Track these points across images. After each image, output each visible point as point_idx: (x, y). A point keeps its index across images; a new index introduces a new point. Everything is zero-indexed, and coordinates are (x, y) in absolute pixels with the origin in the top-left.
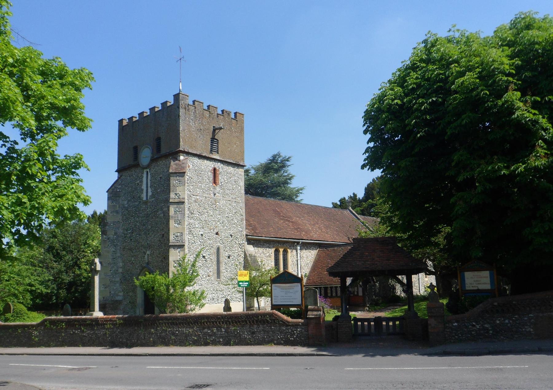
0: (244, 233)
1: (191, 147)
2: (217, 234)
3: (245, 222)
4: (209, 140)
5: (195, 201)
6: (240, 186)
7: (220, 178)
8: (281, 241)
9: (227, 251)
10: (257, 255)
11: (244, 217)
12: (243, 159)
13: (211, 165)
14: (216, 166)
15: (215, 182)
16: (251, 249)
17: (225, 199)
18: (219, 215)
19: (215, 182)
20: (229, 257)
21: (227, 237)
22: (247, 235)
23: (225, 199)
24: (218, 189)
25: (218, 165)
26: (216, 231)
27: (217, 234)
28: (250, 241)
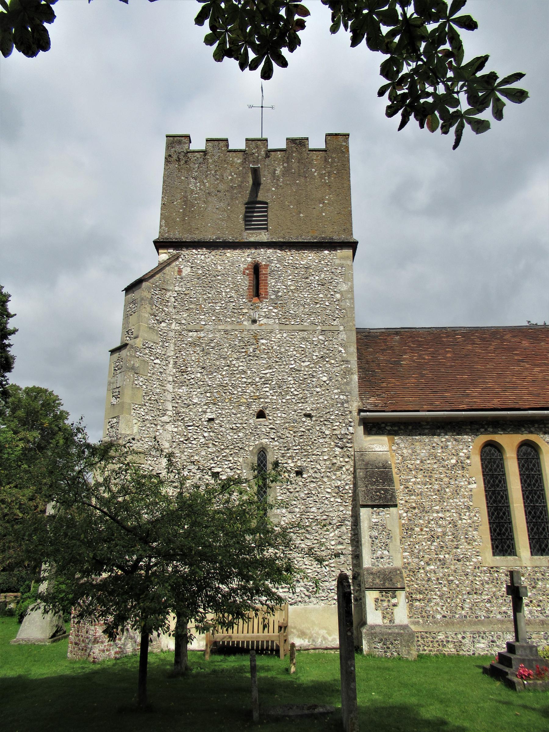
0: (355, 405)
1: (190, 231)
2: (261, 415)
3: (355, 377)
4: (242, 209)
5: (193, 344)
6: (341, 293)
7: (271, 283)
8: (504, 418)
9: (291, 457)
10: (394, 461)
11: (354, 364)
12: (349, 231)
13: (244, 258)
14: (259, 259)
15: (257, 294)
16: (379, 446)
17: (289, 327)
18: (270, 367)
19: (257, 294)
20: (299, 473)
21: (295, 421)
22: (360, 411)
23: (289, 327)
24: (265, 307)
25: (264, 256)
26: (256, 408)
27: (261, 415)
28: (372, 427)
